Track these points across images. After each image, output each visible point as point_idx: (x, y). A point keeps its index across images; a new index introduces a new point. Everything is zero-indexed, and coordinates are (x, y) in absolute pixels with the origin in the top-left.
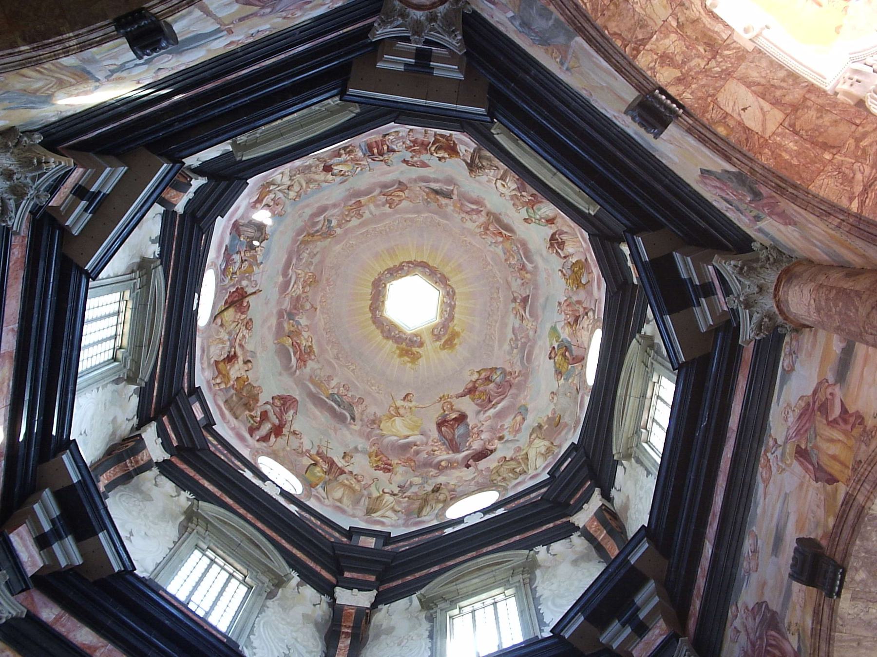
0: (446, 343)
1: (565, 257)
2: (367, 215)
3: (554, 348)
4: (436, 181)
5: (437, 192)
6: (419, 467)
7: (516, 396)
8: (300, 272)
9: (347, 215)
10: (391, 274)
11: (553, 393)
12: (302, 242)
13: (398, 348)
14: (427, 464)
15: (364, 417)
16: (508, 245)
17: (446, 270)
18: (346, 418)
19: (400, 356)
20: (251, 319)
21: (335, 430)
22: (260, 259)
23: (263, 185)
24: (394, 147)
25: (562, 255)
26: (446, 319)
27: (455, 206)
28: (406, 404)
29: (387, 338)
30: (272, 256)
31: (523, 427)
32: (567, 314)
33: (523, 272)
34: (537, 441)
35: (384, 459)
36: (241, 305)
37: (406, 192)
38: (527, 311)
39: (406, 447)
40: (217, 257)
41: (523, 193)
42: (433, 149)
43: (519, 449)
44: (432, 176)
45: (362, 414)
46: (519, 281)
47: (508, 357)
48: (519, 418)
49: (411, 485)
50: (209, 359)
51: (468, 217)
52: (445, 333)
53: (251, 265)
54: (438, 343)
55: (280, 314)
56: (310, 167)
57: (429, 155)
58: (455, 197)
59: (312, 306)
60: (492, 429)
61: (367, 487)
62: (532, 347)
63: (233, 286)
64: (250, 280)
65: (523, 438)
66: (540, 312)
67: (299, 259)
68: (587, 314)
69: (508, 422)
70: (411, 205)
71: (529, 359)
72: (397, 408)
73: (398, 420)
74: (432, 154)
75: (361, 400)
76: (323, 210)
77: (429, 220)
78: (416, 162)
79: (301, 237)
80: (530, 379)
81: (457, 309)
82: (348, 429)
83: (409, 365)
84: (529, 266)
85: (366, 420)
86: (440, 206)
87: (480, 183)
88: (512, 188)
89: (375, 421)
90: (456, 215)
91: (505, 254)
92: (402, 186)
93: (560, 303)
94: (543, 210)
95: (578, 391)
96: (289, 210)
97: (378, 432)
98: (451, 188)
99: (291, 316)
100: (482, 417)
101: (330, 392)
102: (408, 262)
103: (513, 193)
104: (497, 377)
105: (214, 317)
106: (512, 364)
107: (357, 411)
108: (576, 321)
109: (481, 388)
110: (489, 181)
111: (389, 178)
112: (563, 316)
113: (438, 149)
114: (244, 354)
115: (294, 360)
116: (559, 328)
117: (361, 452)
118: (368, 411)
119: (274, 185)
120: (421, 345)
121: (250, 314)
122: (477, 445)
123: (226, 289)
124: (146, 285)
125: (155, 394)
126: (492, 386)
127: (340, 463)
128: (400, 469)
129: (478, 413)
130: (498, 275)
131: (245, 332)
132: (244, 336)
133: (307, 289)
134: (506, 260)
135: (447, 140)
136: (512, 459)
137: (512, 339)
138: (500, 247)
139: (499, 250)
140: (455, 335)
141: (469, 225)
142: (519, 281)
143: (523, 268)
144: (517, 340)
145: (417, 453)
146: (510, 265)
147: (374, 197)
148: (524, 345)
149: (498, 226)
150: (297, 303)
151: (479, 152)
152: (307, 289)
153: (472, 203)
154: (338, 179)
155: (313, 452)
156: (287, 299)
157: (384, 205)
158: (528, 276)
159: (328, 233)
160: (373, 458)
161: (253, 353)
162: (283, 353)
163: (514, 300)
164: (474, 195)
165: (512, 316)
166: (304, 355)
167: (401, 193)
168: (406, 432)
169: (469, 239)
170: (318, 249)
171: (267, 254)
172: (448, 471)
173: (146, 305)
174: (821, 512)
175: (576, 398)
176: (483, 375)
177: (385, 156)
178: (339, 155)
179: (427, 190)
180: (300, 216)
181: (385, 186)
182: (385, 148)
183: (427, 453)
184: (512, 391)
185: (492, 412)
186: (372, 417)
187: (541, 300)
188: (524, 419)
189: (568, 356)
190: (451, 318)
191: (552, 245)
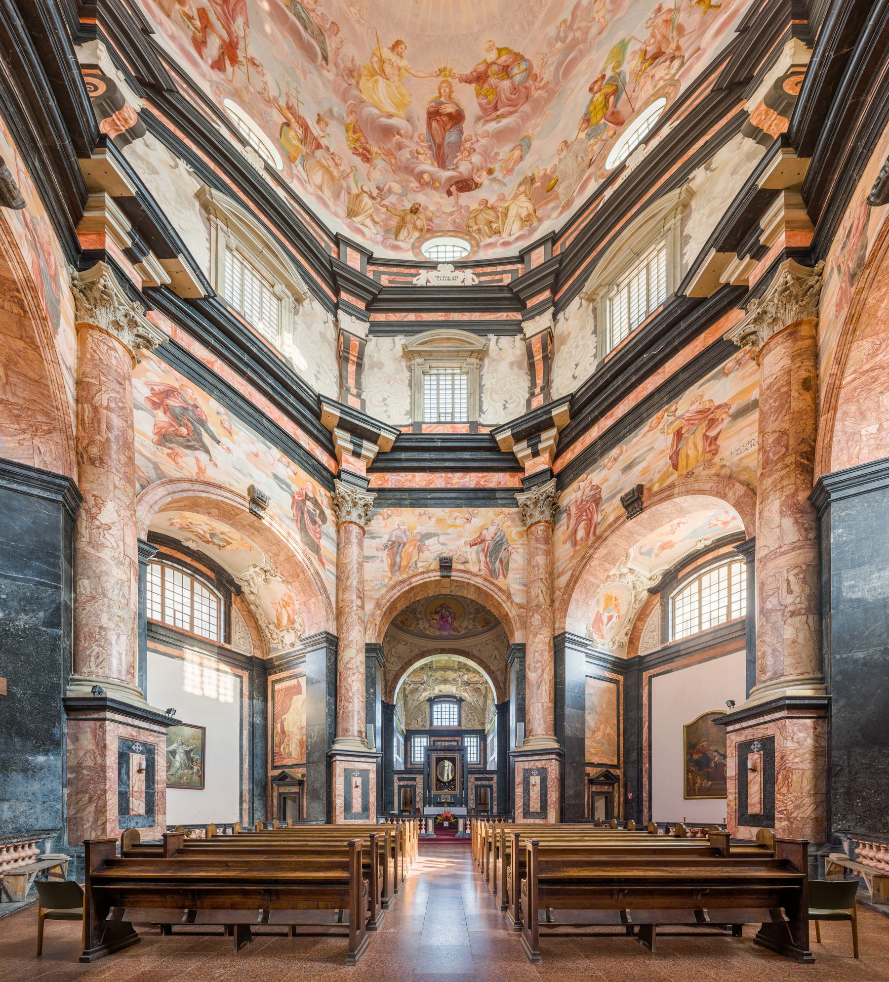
7: (526, 118)
15: (339, 61)
18: (316, 55)
21: (305, 74)
31: (517, 168)
35: (363, 140)
39: (388, 132)
45: (337, 55)
48: (517, 153)
49: (390, 191)
62: (582, 54)
69: (505, 151)
80: (554, 102)
82: (321, 75)
100: (481, 128)
107: (331, 44)
117: (337, 119)
122: (464, 168)
128: (380, 163)
129: (479, 119)
144: (570, 27)
145: (400, 147)
148: (575, 43)
160: (350, 133)
168: (391, 109)
172: (429, 190)
174: (657, 477)
183: (411, 152)
184: (526, 108)
185: (492, 126)
189: (610, 107)
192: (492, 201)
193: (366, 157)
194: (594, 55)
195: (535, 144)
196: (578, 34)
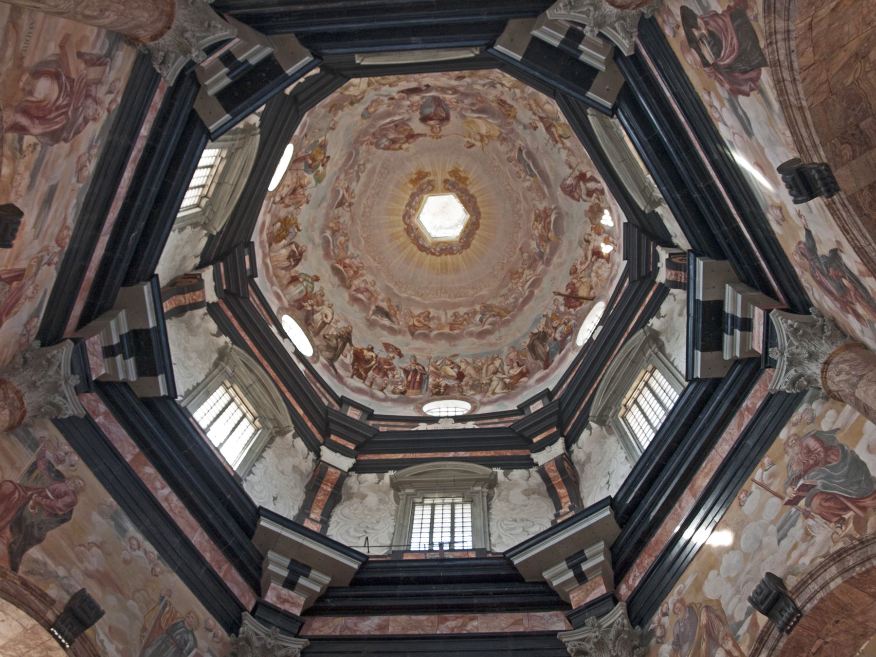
0: (424, 177)
1: (291, 243)
2: (450, 313)
3: (323, 165)
4: (383, 327)
5: (387, 315)
6: (473, 95)
7: (371, 126)
8: (520, 288)
9: (465, 320)
10: (451, 248)
11: (333, 129)
12: (508, 312)
13: (467, 185)
14: (465, 95)
16: (342, 254)
17: (404, 238)
19: (466, 179)
20: (571, 274)
22: (543, 321)
23: (513, 389)
24: (403, 375)
25: (293, 246)
26: (418, 195)
27: (376, 299)
28: (473, 141)
29: (473, 196)
30: (534, 316)
32: (303, 194)
33: (336, 228)
34: (357, 93)
36: (572, 292)
37: (411, 323)
38: (340, 196)
40: (569, 350)
41: (309, 308)
42: (373, 362)
43: (375, 90)
44: (385, 333)
46: (341, 220)
47: (370, 157)
48: (372, 110)
50: (611, 268)
51: (369, 286)
52: (423, 186)
53: (552, 320)
54: (431, 178)
55: (548, 263)
56: (473, 387)
57: (380, 356)
58: (373, 307)
59: (522, 253)
60: (399, 106)
61: (524, 99)
62: (344, 165)
63: (570, 313)
64: (558, 308)
65: (371, 95)
66: (329, 195)
67: (516, 299)
68: (282, 198)
69: (383, 108)
70: (412, 308)
71: (350, 155)
72: (482, 141)
73: (484, 131)
74: (377, 356)
75: (510, 160)
76: (481, 335)
77: (403, 289)
78: (392, 352)
79: (508, 317)
81: (406, 202)
82: (527, 145)
83: (461, 169)
84: (328, 234)
85: (510, 144)
86: (389, 300)
87: (346, 320)
88: (319, 314)
89: (503, 139)
90: (378, 289)
91: (347, 246)
92: (412, 330)
93: (308, 202)
94: (298, 291)
95: (306, 135)
96: (506, 348)
97: (503, 131)
98: (374, 317)
99: (541, 255)
100: (406, 116)
101: (532, 179)
102: (433, 254)
103: (320, 308)
104: (385, 142)
105: (593, 300)
106: (368, 151)
107: (515, 154)
108: (294, 192)
109: (402, 136)
110: (337, 321)
111: (420, 343)
112: (306, 193)
113: (368, 361)
114: (586, 250)
115: (553, 217)
116: (314, 182)
118: (506, 150)
119: (505, 383)
120: (446, 181)
121: (569, 279)
122: (416, 98)
123: (576, 315)
124: (606, 408)
125: (651, 293)
126: (392, 136)
127: (540, 125)
128: (491, 97)
129: (409, 120)
130: (359, 228)
131: (579, 267)
132: (581, 264)
133: (520, 270)
134: (348, 240)
135: (358, 370)
136: (384, 85)
137: (363, 172)
138: (349, 253)
139: (351, 250)
140: (413, 182)
141: (369, 278)
142: (341, 220)
143: (334, 232)
144: (357, 172)
145: (473, 104)
146: (346, 235)
147: (438, 329)
148: (352, 167)
149: (344, 274)
150: (532, 266)
151: (335, 355)
152: (520, 270)
153: (360, 300)
154: (457, 360)
155: (560, 145)
156: (538, 272)
157: (433, 318)
158: (331, 225)
159: (487, 309)
160: (512, 114)
161: (580, 244)
162: (559, 230)
163: (350, 205)
164: (356, 307)
165: (357, 192)
166: (543, 216)
167: (416, 323)
169: (374, 264)
170: (500, 299)
171: (537, 321)
173: (614, 392)
175: (309, 129)
176: (397, 146)
177: (413, 368)
178: (447, 386)
179: (394, 319)
180: (500, 338)
181: (425, 337)
182: (410, 377)
184: (372, 130)
185: (396, 118)
186: (504, 143)
187: (325, 204)
188: (367, 109)
190: (413, 196)
191: (301, 254)
192: (386, 88)
193: (502, 103)
194: (336, 169)
195: (359, 117)
196: (351, 171)
